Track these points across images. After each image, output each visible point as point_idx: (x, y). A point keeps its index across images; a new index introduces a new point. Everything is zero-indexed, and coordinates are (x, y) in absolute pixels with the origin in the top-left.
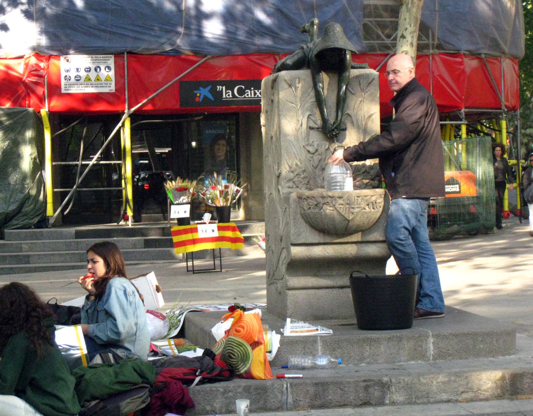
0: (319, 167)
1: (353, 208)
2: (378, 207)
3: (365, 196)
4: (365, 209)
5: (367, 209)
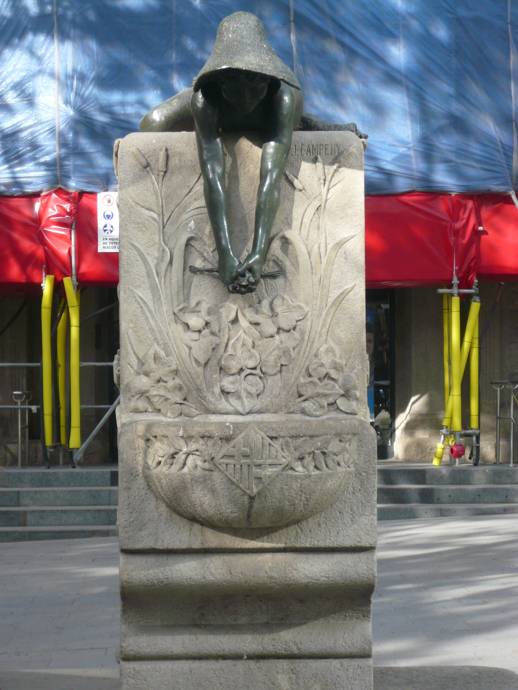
0: (213, 362)
1: (259, 466)
2: (331, 464)
3: (292, 437)
4: (292, 469)
5: (300, 469)
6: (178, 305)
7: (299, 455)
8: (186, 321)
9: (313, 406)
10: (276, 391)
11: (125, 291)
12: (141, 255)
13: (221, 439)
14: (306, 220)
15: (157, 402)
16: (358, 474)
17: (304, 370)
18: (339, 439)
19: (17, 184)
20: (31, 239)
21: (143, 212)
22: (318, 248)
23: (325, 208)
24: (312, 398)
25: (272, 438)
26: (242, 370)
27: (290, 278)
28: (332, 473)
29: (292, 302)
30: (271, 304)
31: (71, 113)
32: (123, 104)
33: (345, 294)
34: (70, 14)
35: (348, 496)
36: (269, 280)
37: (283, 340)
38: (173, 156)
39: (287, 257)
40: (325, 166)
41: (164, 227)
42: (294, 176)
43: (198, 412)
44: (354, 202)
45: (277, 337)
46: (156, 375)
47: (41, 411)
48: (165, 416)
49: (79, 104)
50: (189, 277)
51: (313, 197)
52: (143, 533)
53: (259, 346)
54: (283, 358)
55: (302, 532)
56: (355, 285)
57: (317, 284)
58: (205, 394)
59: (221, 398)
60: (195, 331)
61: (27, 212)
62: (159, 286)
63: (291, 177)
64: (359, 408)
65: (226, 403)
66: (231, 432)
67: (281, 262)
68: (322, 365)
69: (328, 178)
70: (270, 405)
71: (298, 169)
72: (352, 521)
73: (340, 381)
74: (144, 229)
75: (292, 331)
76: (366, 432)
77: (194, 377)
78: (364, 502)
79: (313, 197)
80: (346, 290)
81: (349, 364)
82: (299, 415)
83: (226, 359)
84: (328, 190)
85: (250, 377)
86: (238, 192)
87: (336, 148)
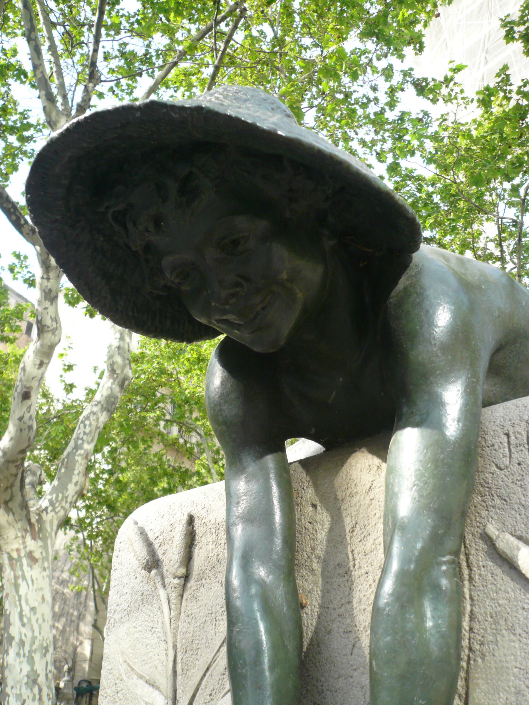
86: (352, 616)
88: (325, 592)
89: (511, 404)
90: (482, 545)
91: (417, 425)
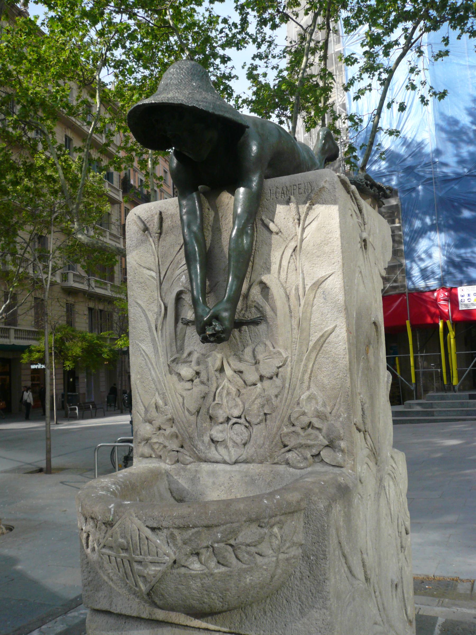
0: (203, 411)
1: (140, 562)
6: (171, 357)
7: (190, 550)
8: (178, 371)
9: (296, 458)
10: (260, 441)
11: (133, 345)
12: (143, 311)
13: (104, 523)
14: (285, 263)
15: (157, 449)
16: (306, 556)
17: (286, 419)
18: (257, 525)
19: (427, 287)
20: (434, 307)
21: (145, 272)
22: (295, 290)
23: (301, 247)
24: (296, 448)
25: (153, 529)
26: (228, 419)
27: (271, 323)
28: (250, 568)
29: (274, 348)
30: (254, 351)
31: (445, 258)
32: (465, 253)
33: (326, 336)
34: (442, 223)
35: (296, 582)
36: (252, 327)
37: (266, 388)
38: (167, 218)
39: (268, 302)
40: (299, 206)
41: (161, 284)
42: (271, 220)
43: (191, 460)
44: (330, 238)
45: (259, 385)
46: (157, 423)
47: (442, 371)
48: (165, 463)
49: (448, 254)
50: (182, 328)
51: (289, 239)
52: (100, 594)
53: (243, 394)
54: (266, 406)
55: (246, 618)
56: (336, 326)
57: (296, 327)
58: (196, 443)
59: (210, 448)
60: (189, 381)
61: (432, 297)
62: (157, 339)
63: (267, 221)
64: (344, 461)
65: (215, 452)
66: (111, 517)
67: (262, 307)
68: (304, 414)
69: (302, 218)
70: (255, 455)
71: (274, 213)
72: (301, 613)
73: (324, 430)
74: (146, 288)
75: (275, 378)
76: (313, 507)
77: (186, 425)
78: (314, 591)
79: (289, 239)
80: (326, 332)
81: (334, 412)
82: (284, 466)
83: (214, 407)
84: (304, 229)
85: (236, 426)
86: (221, 243)
87: (309, 186)
88: (213, 236)
89: (273, 179)
90: (260, 222)
91: (244, 187)
